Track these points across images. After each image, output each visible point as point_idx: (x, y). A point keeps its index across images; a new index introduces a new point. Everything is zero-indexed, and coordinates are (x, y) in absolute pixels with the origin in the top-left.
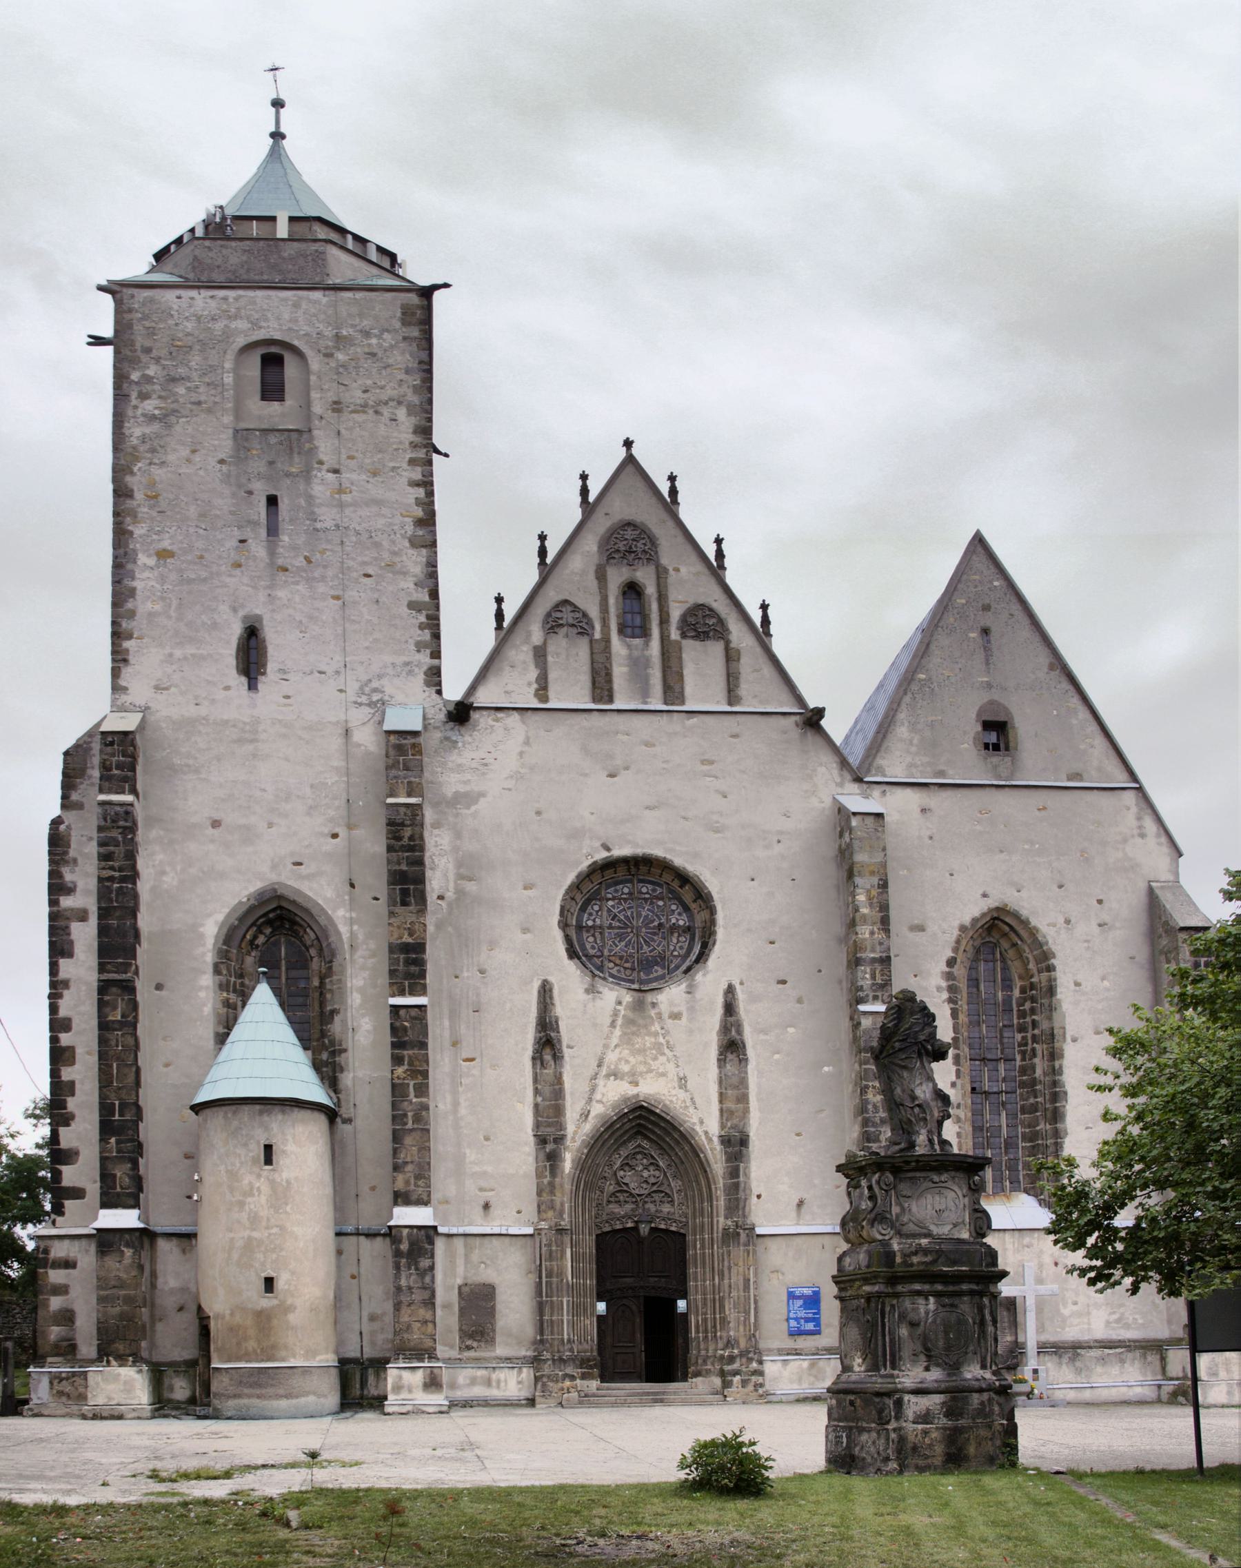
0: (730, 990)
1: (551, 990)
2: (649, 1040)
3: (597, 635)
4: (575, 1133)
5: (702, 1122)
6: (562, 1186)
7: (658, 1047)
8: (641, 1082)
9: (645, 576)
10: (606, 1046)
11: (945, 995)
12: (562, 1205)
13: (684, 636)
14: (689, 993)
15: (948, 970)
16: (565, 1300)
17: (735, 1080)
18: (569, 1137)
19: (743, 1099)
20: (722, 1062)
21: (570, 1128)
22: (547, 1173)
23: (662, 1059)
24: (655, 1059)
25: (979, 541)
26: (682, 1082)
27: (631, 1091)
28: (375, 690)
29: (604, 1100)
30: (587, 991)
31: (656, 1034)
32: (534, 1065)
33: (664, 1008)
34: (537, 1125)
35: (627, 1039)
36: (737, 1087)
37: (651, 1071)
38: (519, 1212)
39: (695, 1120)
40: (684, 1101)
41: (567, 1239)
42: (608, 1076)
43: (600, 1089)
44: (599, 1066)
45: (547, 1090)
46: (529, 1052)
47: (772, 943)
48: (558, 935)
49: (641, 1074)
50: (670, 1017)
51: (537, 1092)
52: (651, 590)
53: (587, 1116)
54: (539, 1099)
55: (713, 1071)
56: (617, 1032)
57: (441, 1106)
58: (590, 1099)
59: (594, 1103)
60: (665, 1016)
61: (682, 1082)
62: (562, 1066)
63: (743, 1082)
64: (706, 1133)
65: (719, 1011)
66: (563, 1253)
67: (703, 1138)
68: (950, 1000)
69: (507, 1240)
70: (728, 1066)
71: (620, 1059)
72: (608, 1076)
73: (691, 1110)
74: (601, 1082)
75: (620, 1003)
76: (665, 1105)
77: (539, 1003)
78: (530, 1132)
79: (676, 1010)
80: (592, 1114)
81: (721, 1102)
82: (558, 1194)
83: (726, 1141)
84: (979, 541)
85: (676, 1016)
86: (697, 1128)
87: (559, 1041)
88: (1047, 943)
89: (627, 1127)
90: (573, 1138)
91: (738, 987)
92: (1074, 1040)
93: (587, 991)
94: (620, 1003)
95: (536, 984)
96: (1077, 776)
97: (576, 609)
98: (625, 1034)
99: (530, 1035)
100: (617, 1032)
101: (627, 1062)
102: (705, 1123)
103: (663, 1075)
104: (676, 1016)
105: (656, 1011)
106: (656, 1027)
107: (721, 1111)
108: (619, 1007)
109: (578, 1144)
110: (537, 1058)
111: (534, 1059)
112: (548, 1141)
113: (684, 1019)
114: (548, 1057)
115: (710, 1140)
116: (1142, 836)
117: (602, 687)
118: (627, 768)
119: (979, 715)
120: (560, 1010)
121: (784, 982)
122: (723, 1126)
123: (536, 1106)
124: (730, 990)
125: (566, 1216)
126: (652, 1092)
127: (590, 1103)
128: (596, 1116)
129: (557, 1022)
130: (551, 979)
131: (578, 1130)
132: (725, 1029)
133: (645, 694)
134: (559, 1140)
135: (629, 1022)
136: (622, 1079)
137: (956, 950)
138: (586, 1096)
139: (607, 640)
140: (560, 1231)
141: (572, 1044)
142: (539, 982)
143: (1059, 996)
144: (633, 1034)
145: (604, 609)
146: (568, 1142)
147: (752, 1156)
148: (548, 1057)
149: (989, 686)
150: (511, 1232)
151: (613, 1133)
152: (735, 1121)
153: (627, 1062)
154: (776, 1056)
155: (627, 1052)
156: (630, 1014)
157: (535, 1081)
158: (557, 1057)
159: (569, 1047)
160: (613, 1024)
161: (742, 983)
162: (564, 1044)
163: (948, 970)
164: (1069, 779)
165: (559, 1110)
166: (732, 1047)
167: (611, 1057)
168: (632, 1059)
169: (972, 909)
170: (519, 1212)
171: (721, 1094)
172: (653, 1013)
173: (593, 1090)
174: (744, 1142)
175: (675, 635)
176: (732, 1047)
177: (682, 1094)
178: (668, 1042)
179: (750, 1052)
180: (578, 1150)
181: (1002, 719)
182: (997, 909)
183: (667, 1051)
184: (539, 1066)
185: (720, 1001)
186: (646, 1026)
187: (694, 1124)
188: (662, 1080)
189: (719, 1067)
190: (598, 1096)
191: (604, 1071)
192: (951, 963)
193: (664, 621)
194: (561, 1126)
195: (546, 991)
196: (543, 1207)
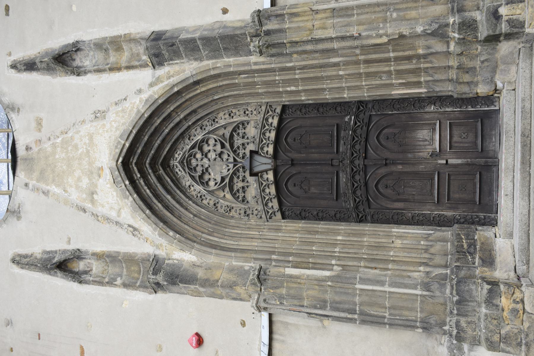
1: (20, 256)
2: (60, 155)
4: (153, 244)
5: (140, 91)
6: (209, 268)
7: (65, 142)
8: (98, 164)
12: (231, 270)
14: (18, 111)
16: (358, 286)
17: (99, 56)
18: (157, 252)
20: (78, 72)
21: (148, 249)
22: (192, 287)
23: (76, 141)
24: (76, 147)
27: (107, 175)
29: (116, 207)
30: (19, 218)
31: (54, 146)
32: (87, 282)
34: (143, 287)
36: (106, 50)
37: (88, 152)
38: (243, 324)
40: (117, 113)
41: (273, 271)
42: (93, 201)
44: (84, 211)
45: (112, 270)
46: (75, 285)
49: (90, 164)
50: (40, 130)
51: (111, 283)
53: (135, 229)
54: (119, 281)
55: (90, 79)
56: (54, 189)
58: (117, 223)
59: (120, 220)
60: (38, 135)
61: (99, 115)
62: (86, 252)
63: (100, 46)
64: (151, 85)
65: (34, 76)
66: (291, 276)
67: (156, 88)
69: (276, 346)
71: (77, 187)
72: (93, 201)
73: (127, 105)
75: (26, 185)
76: (121, 136)
77: (28, 269)
79: (34, 124)
80: (132, 222)
81: (119, 69)
82: (217, 274)
83: (158, 59)
85: (39, 123)
86: (145, 96)
87: (64, 252)
89: (153, 179)
90: (158, 247)
91: (12, 58)
93: (19, 218)
94: (26, 185)
95: (16, 270)
99: (59, 282)
100: (54, 189)
103: (91, 137)
104: (39, 123)
105: (33, 146)
106: (47, 146)
107: (129, 68)
108: (30, 186)
109: (163, 241)
110: (78, 277)
111: (80, 282)
112: (164, 277)
113: (42, 115)
114: (81, 266)
120: (36, 249)
121: (7, 8)
122: (144, 66)
123: (125, 285)
125: (247, 266)
126: (107, 152)
128: (133, 217)
129: (49, 252)
130: (10, 255)
131: (147, 239)
132: (48, 70)
134: (156, 264)
136: (96, 186)
138: (115, 227)
140: (261, 277)
141: (66, 240)
142: (14, 266)
144: (53, 171)
146: (161, 253)
147: (177, 25)
148: (81, 266)
150: (266, 340)
151: (157, 196)
152: (141, 49)
153: (79, 179)
154: (74, 8)
155: (70, 180)
156: (36, 174)
157: (100, 283)
158: (78, 255)
159: (69, 242)
160: (46, 193)
161: (10, 54)
165: (130, 260)
167: (75, 196)
168: (78, 173)
170: (243, 324)
171: (111, 69)
172: (35, 149)
173: (108, 219)
174: (157, 37)
177: (111, 116)
179: (70, 39)
180: (171, 243)
183: (70, 134)
186: (47, 158)
189: (85, 73)
190: (113, 214)
191: (88, 205)
194: (145, 259)
195: (22, 261)
196: (234, 295)
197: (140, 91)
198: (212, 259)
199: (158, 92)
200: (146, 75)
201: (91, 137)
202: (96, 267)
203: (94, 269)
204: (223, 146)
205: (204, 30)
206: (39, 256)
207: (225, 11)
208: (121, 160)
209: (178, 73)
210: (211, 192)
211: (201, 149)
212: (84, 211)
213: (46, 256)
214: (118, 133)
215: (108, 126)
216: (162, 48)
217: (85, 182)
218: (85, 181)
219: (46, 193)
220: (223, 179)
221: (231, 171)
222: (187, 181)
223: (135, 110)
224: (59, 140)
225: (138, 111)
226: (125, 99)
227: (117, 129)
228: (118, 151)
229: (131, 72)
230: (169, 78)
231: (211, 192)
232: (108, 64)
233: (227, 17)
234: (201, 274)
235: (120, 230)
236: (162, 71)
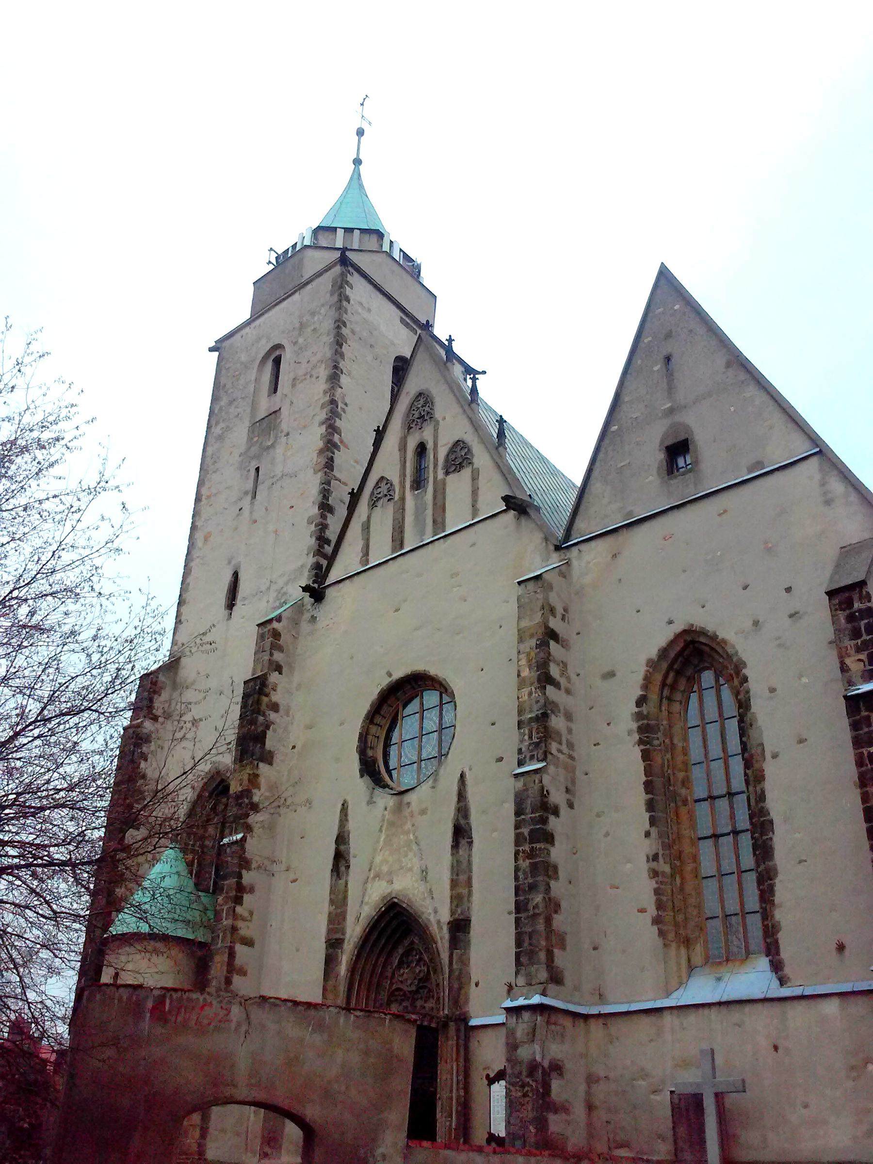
0: (462, 776)
3: (397, 497)
4: (351, 937)
5: (436, 912)
9: (427, 435)
10: (375, 850)
11: (636, 737)
13: (447, 473)
14: (433, 787)
15: (637, 710)
18: (346, 941)
19: (469, 883)
24: (406, 856)
25: (664, 277)
26: (424, 872)
28: (285, 593)
33: (415, 806)
34: (329, 931)
35: (388, 842)
37: (402, 868)
39: (430, 911)
42: (374, 877)
43: (369, 891)
44: (370, 870)
46: (330, 867)
47: (493, 724)
48: (355, 758)
51: (332, 902)
52: (430, 446)
57: (274, 924)
58: (362, 902)
64: (439, 922)
65: (455, 799)
68: (641, 742)
70: (461, 852)
73: (428, 901)
74: (369, 885)
76: (409, 900)
78: (324, 940)
79: (424, 806)
84: (664, 277)
85: (423, 812)
86: (432, 918)
87: (348, 853)
88: (737, 652)
89: (395, 923)
92: (775, 756)
94: (386, 809)
95: (339, 806)
96: (759, 464)
97: (388, 482)
98: (387, 836)
101: (387, 862)
102: (436, 913)
103: (410, 870)
106: (408, 826)
113: (429, 812)
115: (441, 928)
116: (828, 502)
117: (398, 540)
118: (405, 601)
119: (662, 441)
120: (352, 825)
122: (452, 913)
123: (330, 913)
124: (462, 776)
127: (364, 904)
130: (349, 799)
131: (353, 931)
133: (422, 533)
135: (391, 824)
137: (645, 687)
139: (403, 499)
143: (752, 710)
145: (403, 475)
148: (343, 869)
149: (671, 411)
151: (384, 929)
154: (495, 834)
160: (381, 830)
162: (351, 856)
163: (637, 710)
164: (750, 472)
166: (461, 833)
167: (378, 859)
169: (660, 637)
171: (452, 880)
173: (364, 895)
175: (441, 475)
176: (461, 833)
177: (422, 887)
178: (416, 838)
181: (682, 438)
182: (685, 632)
183: (414, 847)
184: (334, 878)
185: (455, 789)
187: (430, 914)
188: (409, 875)
189: (452, 854)
190: (366, 899)
192: (641, 701)
193: (436, 465)
197: (436, 912)
198: (342, 988)
199: (434, 929)
200: (445, 916)
201: (410, 870)
202: (342, 882)
203: (340, 882)
204: (420, 980)
205: (461, 970)
206: (346, 829)
207: (477, 985)
208: (396, 900)
209: (443, 947)
210: (393, 974)
211: (421, 959)
212: (370, 870)
213: (346, 834)
214: (411, 896)
215: (416, 885)
216: (460, 927)
217: (385, 868)
218: (385, 868)
219: (381, 830)
220: (401, 982)
221: (405, 988)
222: (401, 951)
223: (424, 910)
224: (411, 837)
225: (423, 913)
226: (432, 898)
227: (414, 895)
228: (401, 898)
229: (449, 900)
230: (441, 939)
231: (393, 974)
232: (457, 875)
233: (473, 985)
234: (331, 983)
235: (358, 905)
236: (445, 929)
